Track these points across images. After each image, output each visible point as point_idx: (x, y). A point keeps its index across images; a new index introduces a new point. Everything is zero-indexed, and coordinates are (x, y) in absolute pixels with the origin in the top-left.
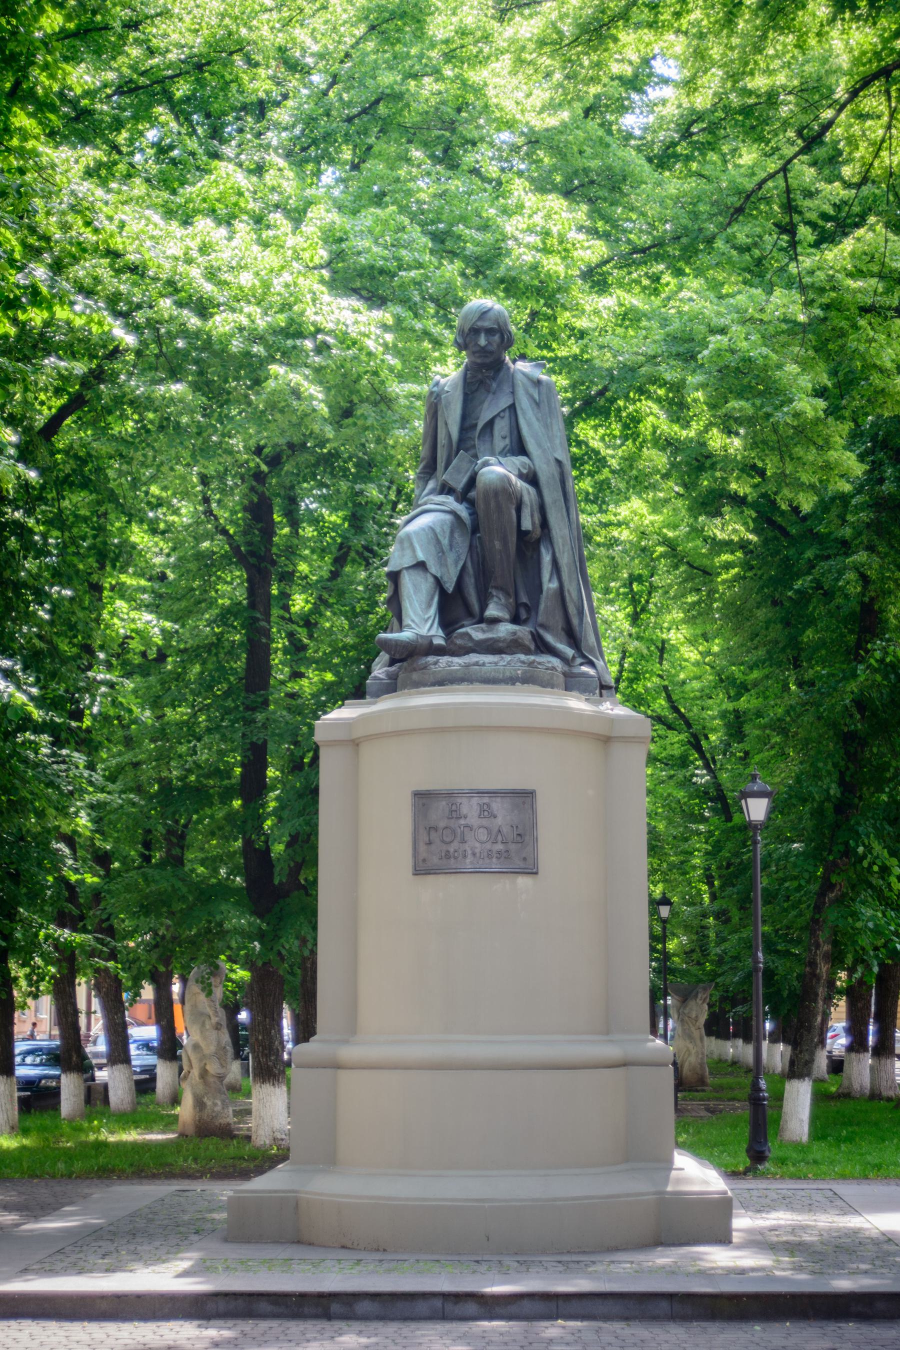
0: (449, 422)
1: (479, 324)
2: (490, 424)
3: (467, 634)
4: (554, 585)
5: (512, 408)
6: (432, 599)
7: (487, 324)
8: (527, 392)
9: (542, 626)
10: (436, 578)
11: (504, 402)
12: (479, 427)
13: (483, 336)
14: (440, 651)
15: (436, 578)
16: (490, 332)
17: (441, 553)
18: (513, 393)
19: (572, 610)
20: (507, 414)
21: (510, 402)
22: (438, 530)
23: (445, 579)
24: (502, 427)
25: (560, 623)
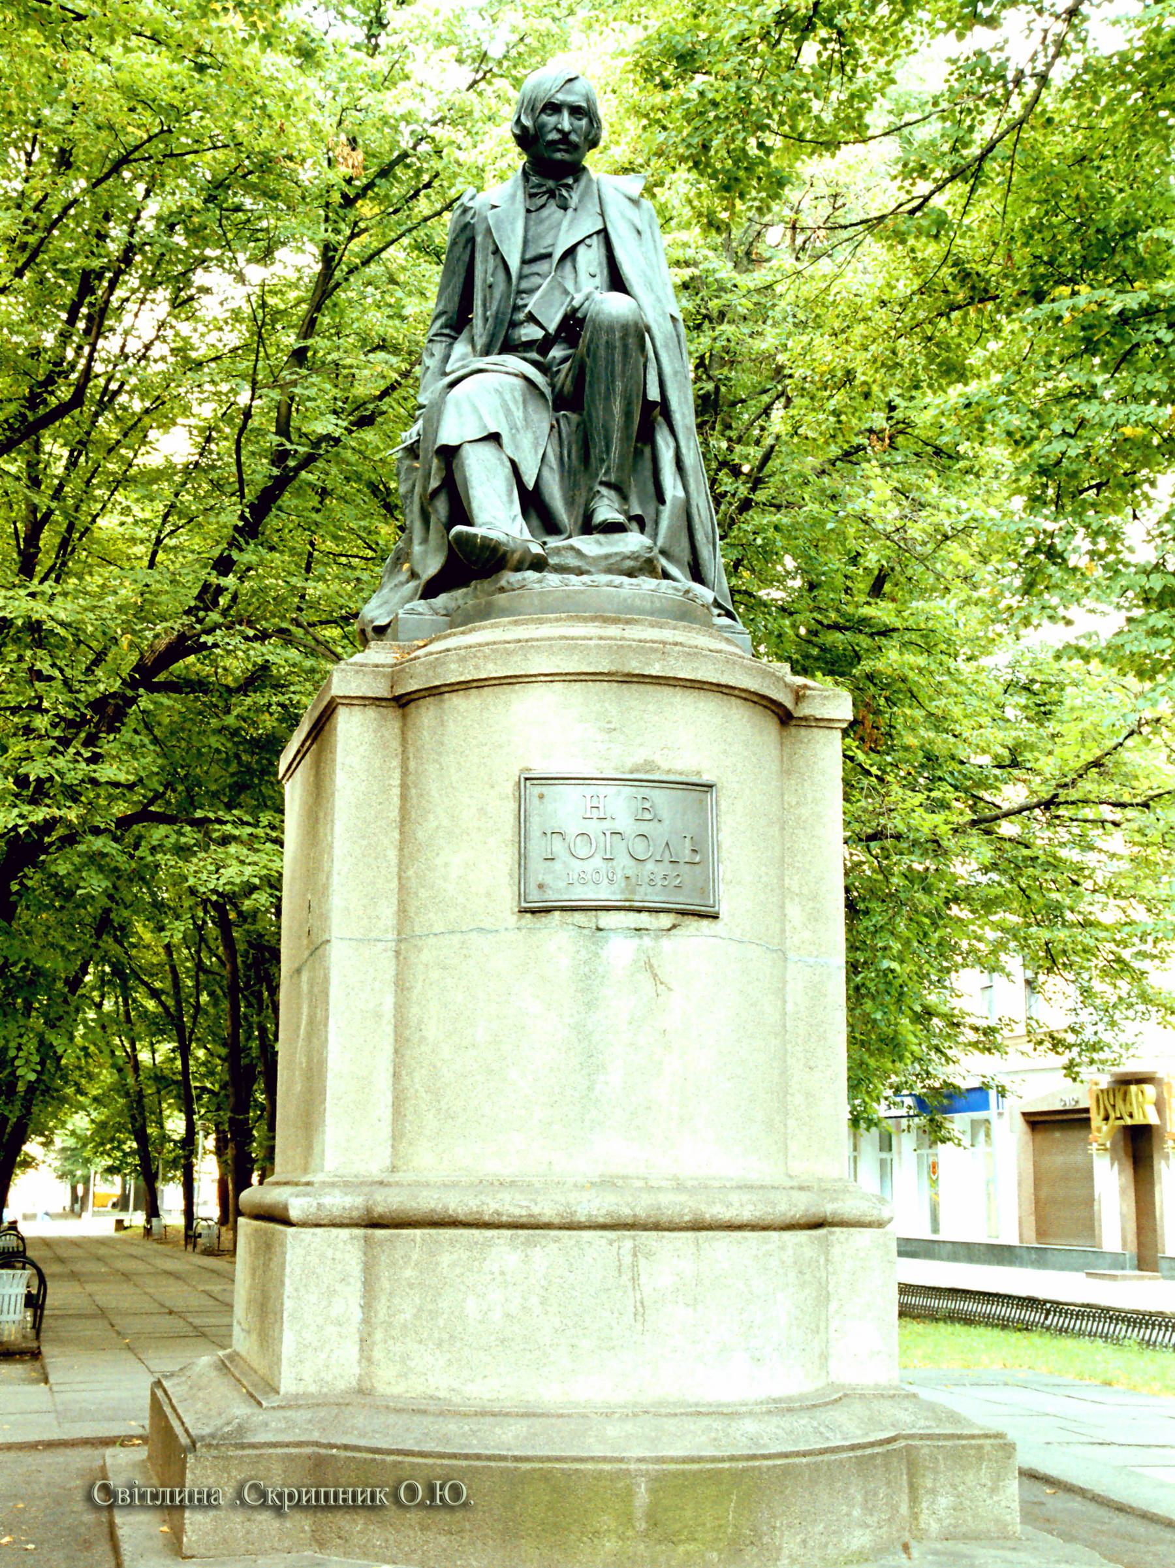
0: (504, 249)
1: (560, 97)
2: (571, 253)
3: (572, 548)
4: (681, 494)
5: (604, 233)
6: (511, 491)
7: (571, 99)
8: (623, 216)
9: (663, 552)
10: (512, 462)
11: (591, 224)
12: (557, 255)
13: (566, 114)
14: (539, 564)
15: (512, 462)
16: (575, 111)
17: (513, 427)
18: (602, 215)
19: (700, 536)
20: (594, 241)
21: (600, 227)
22: (508, 397)
23: (523, 468)
24: (590, 259)
25: (686, 556)
